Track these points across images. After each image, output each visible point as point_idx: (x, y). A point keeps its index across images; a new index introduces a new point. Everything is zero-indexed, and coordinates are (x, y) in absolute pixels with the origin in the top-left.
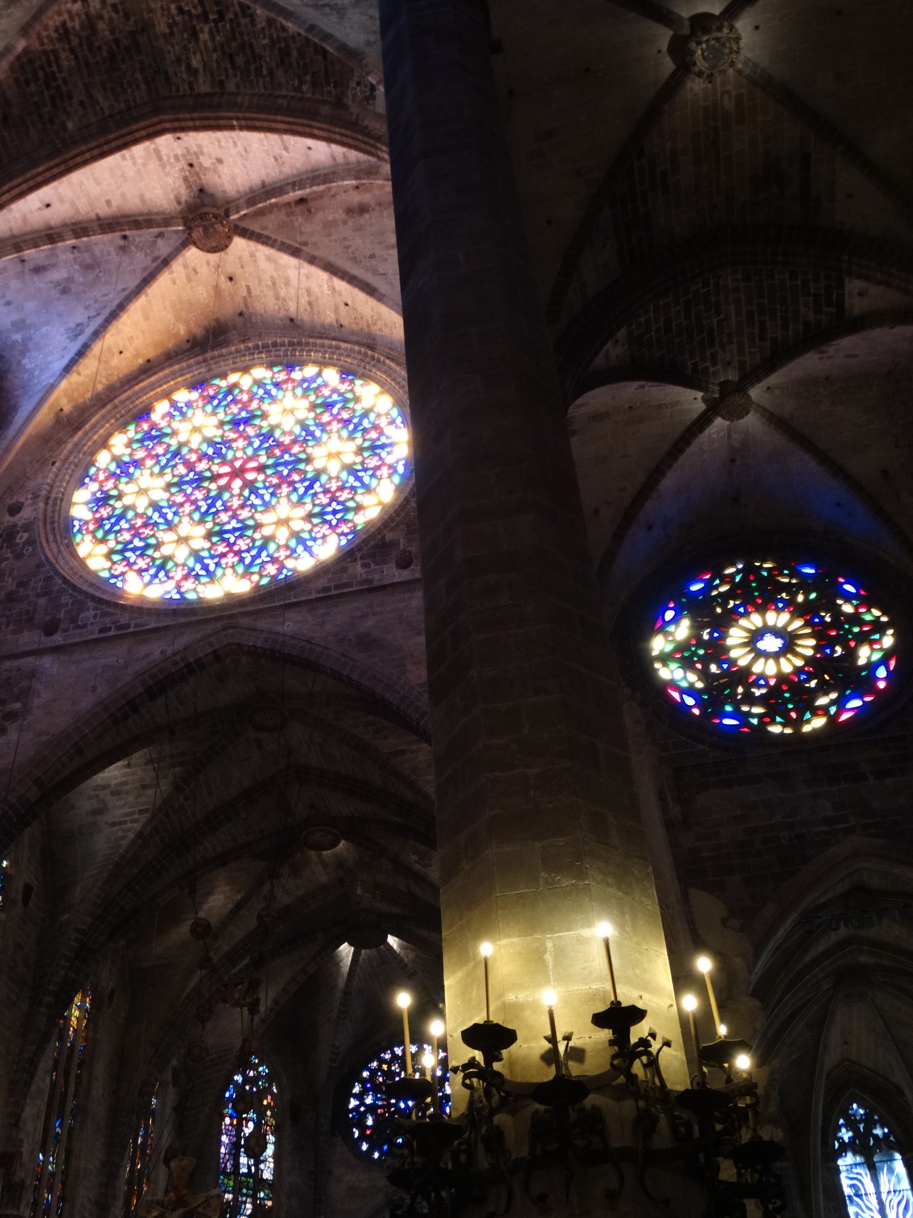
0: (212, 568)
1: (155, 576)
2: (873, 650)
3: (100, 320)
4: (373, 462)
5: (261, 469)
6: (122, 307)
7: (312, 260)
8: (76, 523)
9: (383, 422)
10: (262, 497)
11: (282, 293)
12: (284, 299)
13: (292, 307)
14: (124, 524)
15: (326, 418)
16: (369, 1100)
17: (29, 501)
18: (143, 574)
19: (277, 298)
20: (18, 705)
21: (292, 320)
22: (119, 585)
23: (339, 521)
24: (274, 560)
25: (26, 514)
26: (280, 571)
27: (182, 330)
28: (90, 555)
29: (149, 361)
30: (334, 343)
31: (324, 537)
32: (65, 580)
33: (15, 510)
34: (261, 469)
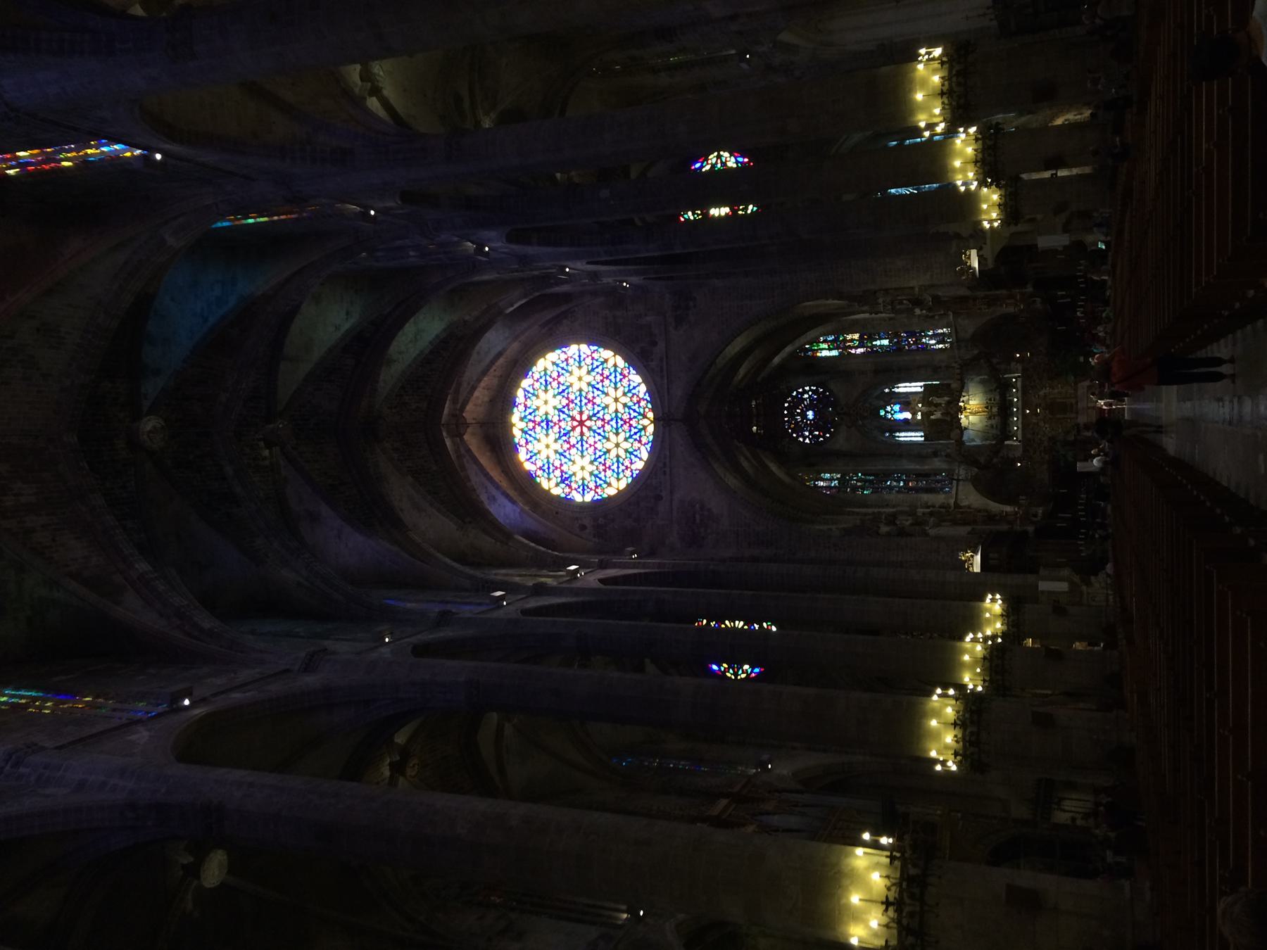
0: (636, 430)
1: (636, 456)
2: (730, 161)
3: (489, 485)
4: (589, 361)
5: (581, 413)
6: (487, 475)
7: (479, 380)
8: (595, 498)
9: (563, 357)
10: (598, 412)
11: (480, 402)
12: (483, 402)
13: (486, 399)
14: (602, 475)
15: (555, 384)
16: (807, 434)
17: (580, 522)
18: (633, 461)
19: (481, 406)
20: (698, 505)
21: (491, 401)
22: (637, 472)
23: (621, 374)
24: (639, 402)
25: (587, 522)
26: (644, 399)
27: (488, 454)
28: (618, 489)
29: (503, 471)
30: (509, 380)
31: (629, 381)
32: (633, 495)
33: (583, 527)
34: (581, 413)
